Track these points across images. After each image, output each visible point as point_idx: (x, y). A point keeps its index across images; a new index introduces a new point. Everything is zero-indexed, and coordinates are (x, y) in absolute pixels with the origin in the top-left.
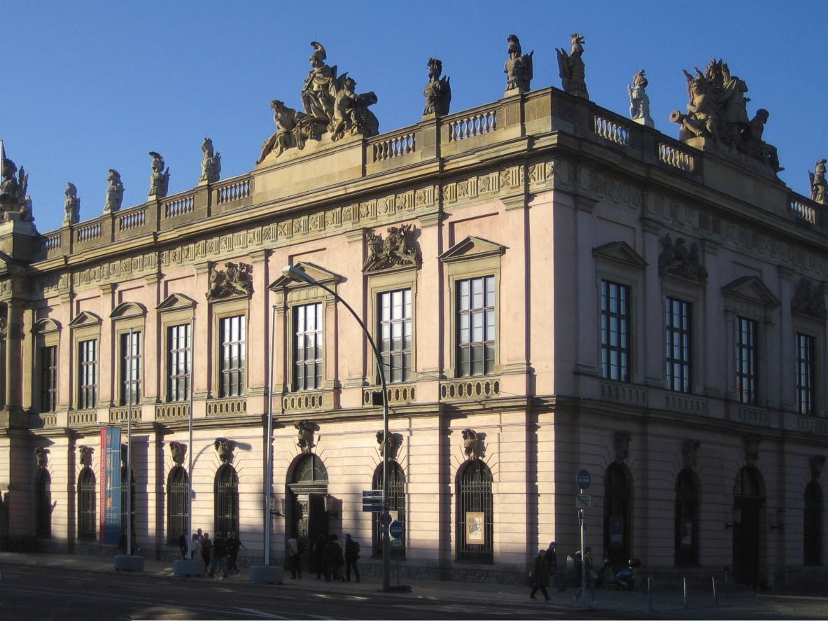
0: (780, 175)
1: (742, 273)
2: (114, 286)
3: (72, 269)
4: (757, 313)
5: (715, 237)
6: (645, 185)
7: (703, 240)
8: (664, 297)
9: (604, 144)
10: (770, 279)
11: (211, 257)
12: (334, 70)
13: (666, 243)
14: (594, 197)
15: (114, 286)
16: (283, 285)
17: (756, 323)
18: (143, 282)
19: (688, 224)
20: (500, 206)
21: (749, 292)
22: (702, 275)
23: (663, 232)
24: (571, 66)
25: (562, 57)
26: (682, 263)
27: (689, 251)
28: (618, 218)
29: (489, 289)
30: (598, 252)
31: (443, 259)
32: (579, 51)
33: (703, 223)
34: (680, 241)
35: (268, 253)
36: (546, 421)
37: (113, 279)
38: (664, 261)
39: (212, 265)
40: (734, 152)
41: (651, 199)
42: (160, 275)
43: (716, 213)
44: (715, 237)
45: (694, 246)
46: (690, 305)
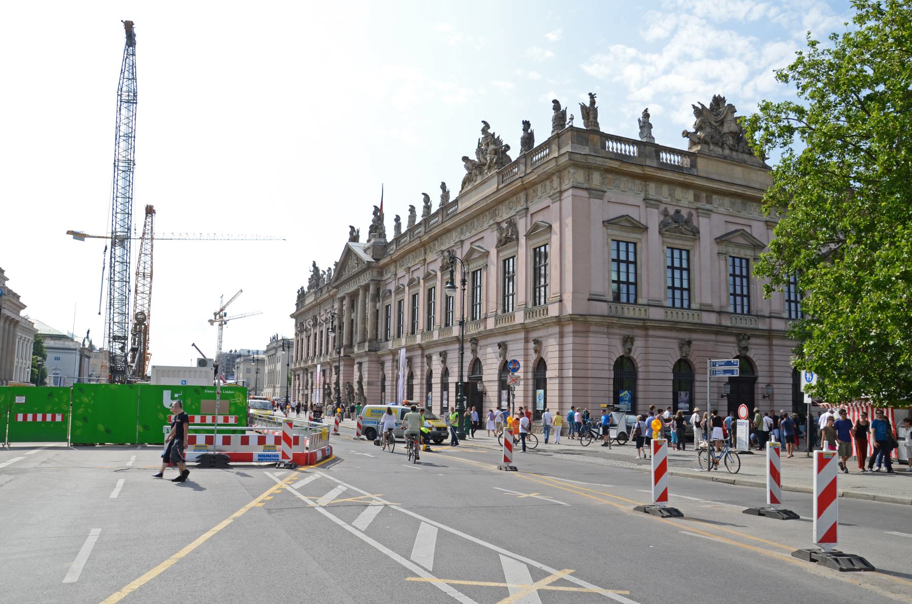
0: (767, 162)
1: (733, 228)
2: (409, 268)
3: (394, 261)
4: (749, 253)
5: (708, 206)
6: (646, 178)
7: (697, 209)
8: (665, 248)
9: (613, 157)
10: (758, 230)
11: (443, 248)
12: (493, 135)
13: (665, 213)
14: (605, 189)
15: (409, 268)
16: (466, 261)
17: (748, 260)
18: (419, 266)
19: (685, 200)
20: (547, 202)
21: (741, 240)
22: (696, 232)
23: (662, 207)
24: (589, 112)
25: (583, 107)
26: (678, 226)
27: (686, 217)
28: (626, 200)
29: (615, 252)
30: (608, 223)
31: (527, 236)
32: (593, 103)
33: (697, 198)
34: (678, 212)
35: (462, 242)
36: (569, 329)
37: (410, 265)
38: (663, 225)
39: (443, 252)
40: (727, 152)
41: (652, 187)
42: (425, 260)
43: (708, 193)
44: (708, 206)
45: (690, 215)
46: (688, 251)
